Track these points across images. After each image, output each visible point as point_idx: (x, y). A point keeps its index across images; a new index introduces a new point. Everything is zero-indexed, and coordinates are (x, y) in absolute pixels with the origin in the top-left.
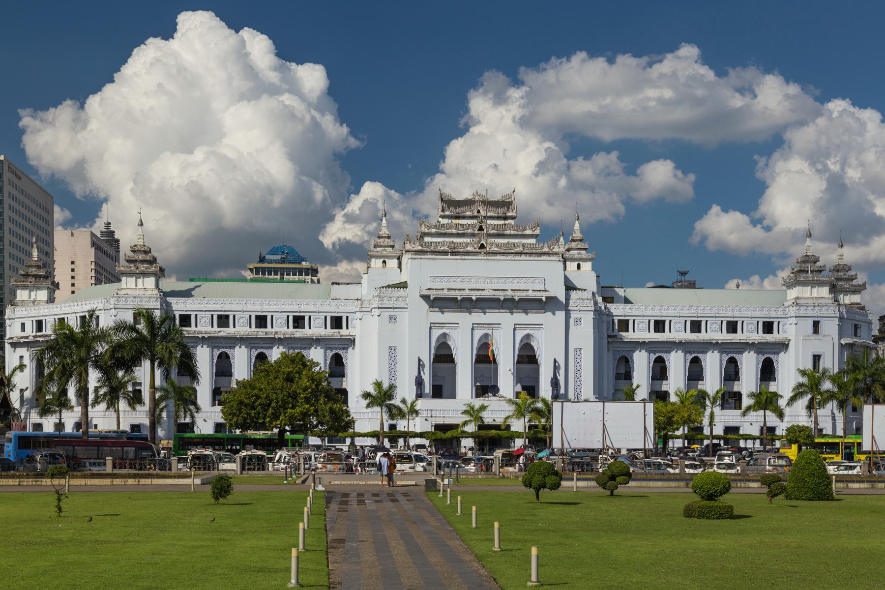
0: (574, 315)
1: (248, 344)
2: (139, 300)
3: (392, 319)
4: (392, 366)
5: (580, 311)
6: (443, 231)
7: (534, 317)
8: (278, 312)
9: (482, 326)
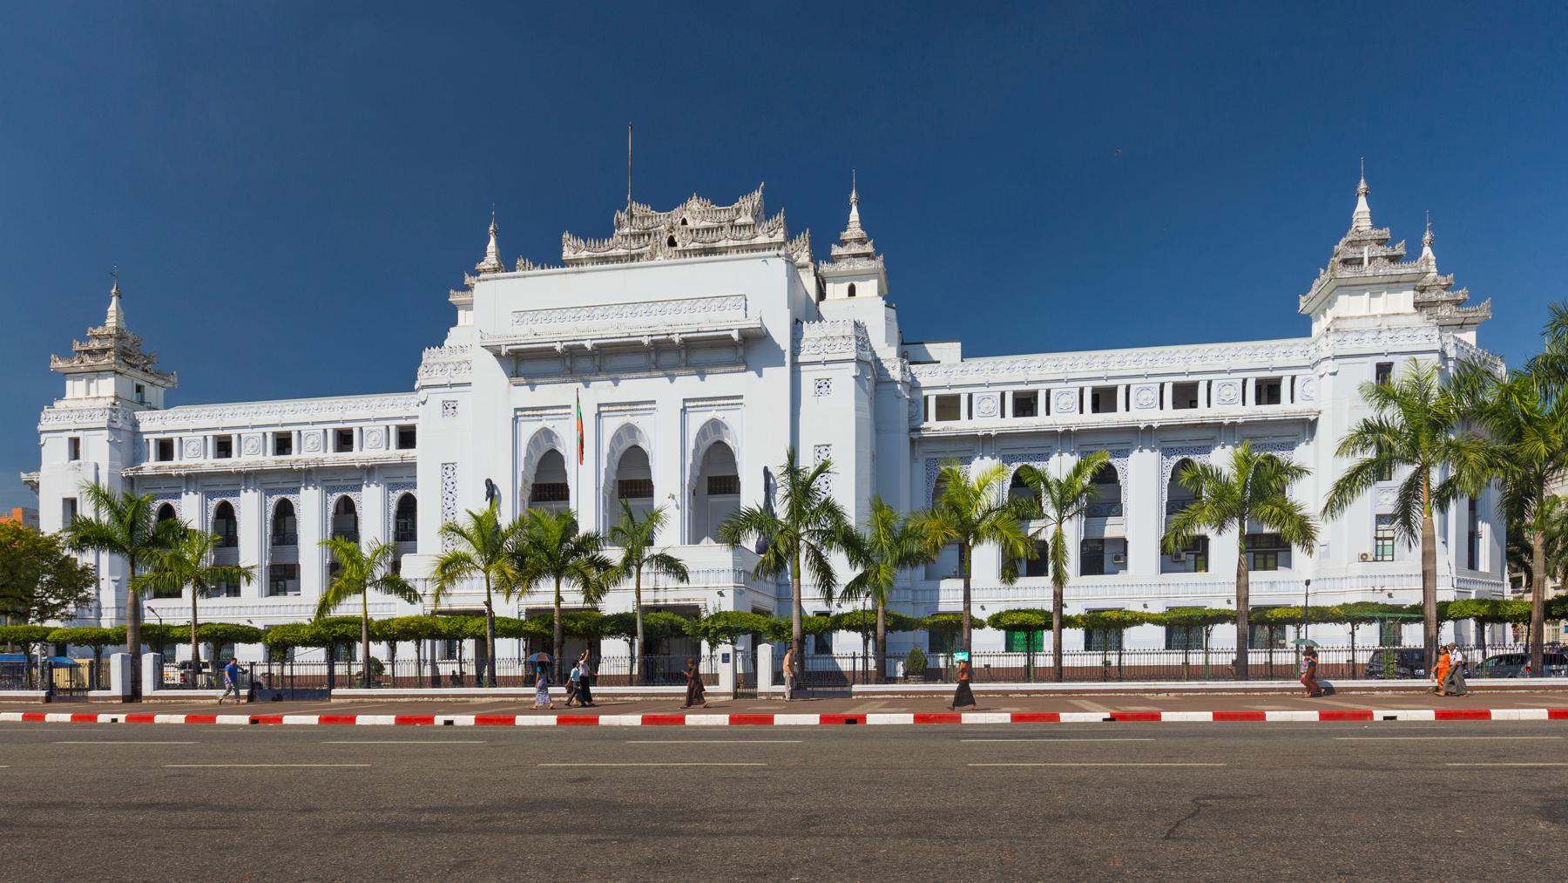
0: (808, 377)
2: (77, 414)
4: (448, 502)
5: (826, 362)
6: (602, 254)
7: (720, 382)
8: (307, 423)
9: (619, 408)
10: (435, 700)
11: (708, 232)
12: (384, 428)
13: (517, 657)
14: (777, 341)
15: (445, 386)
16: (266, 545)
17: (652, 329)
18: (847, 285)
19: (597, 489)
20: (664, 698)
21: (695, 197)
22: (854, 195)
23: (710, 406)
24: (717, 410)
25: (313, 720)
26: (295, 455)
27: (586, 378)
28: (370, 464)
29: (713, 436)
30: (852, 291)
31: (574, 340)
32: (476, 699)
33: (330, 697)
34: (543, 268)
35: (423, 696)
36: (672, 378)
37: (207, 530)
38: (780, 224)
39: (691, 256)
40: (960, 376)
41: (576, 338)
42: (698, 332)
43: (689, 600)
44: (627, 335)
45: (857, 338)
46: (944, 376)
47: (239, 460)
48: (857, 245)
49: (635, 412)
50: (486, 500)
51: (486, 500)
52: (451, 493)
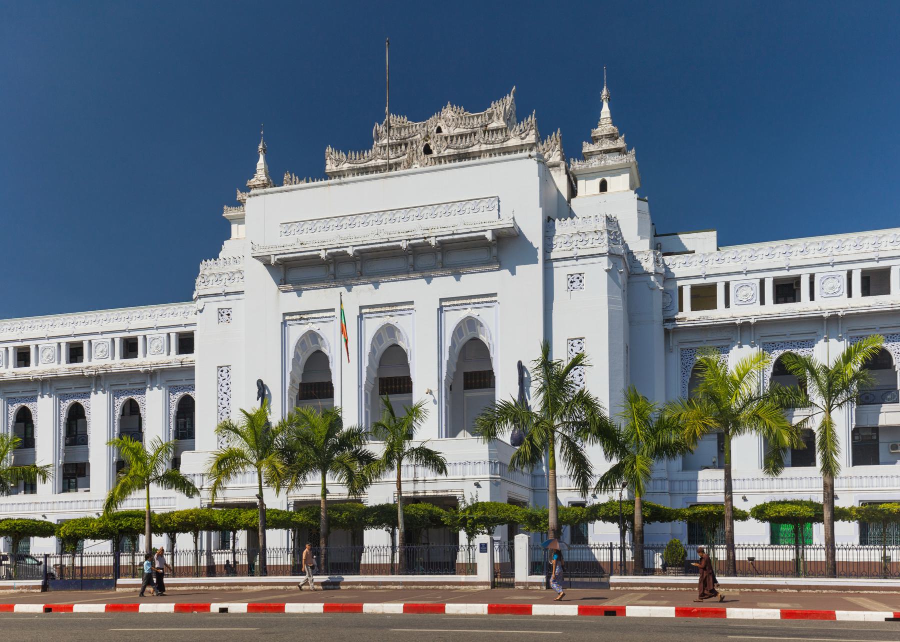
0: (560, 273)
1: (53, 389)
5: (579, 258)
6: (362, 165)
8: (97, 333)
9: (380, 309)
10: (211, 588)
11: (462, 138)
12: (165, 336)
13: (286, 547)
14: (530, 239)
16: (60, 446)
17: (409, 234)
18: (596, 182)
19: (360, 386)
20: (425, 587)
21: (449, 105)
22: (605, 92)
23: (466, 304)
24: (472, 308)
25: (100, 608)
26: (86, 362)
27: (348, 282)
28: (153, 368)
29: (469, 333)
30: (603, 187)
31: (338, 248)
32: (248, 587)
33: (116, 586)
34: (308, 181)
35: (200, 585)
36: (429, 280)
37: (8, 433)
38: (532, 126)
39: (445, 161)
40: (716, 265)
41: (339, 246)
42: (453, 234)
43: (447, 491)
44: (386, 240)
45: (609, 232)
46: (699, 266)
47: (36, 369)
48: (608, 141)
49: (394, 313)
50: (258, 399)
51: (258, 399)
52: (226, 393)
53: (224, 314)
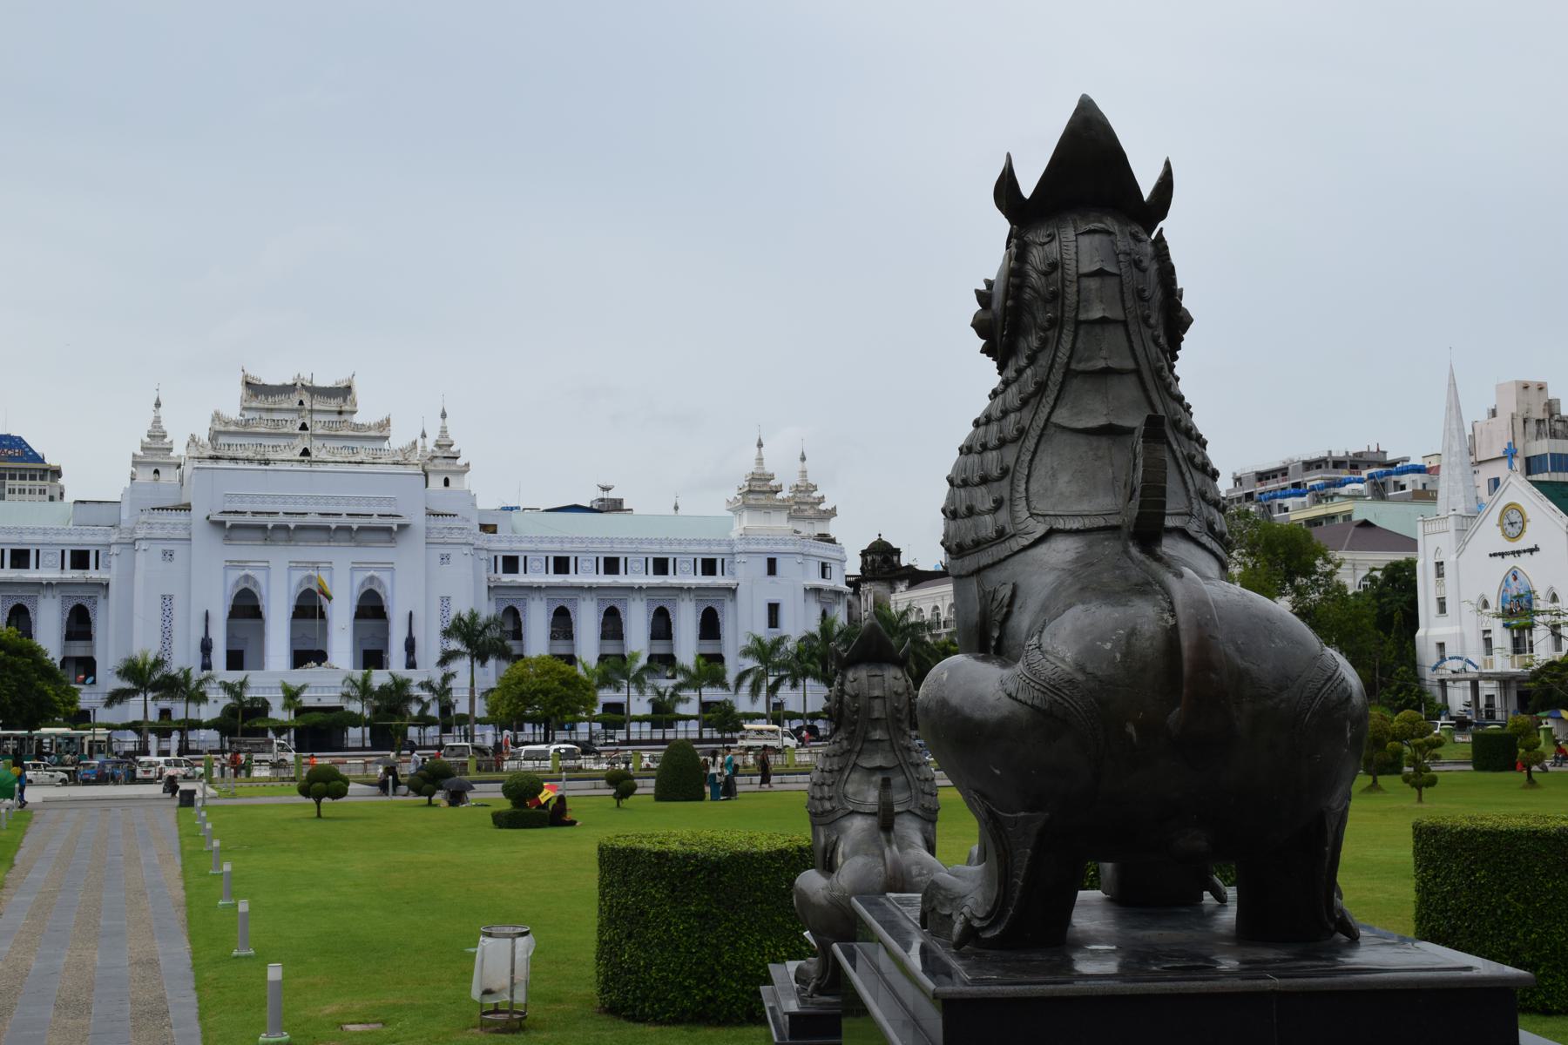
3: (169, 555)
15: (166, 539)
53: (167, 555)
